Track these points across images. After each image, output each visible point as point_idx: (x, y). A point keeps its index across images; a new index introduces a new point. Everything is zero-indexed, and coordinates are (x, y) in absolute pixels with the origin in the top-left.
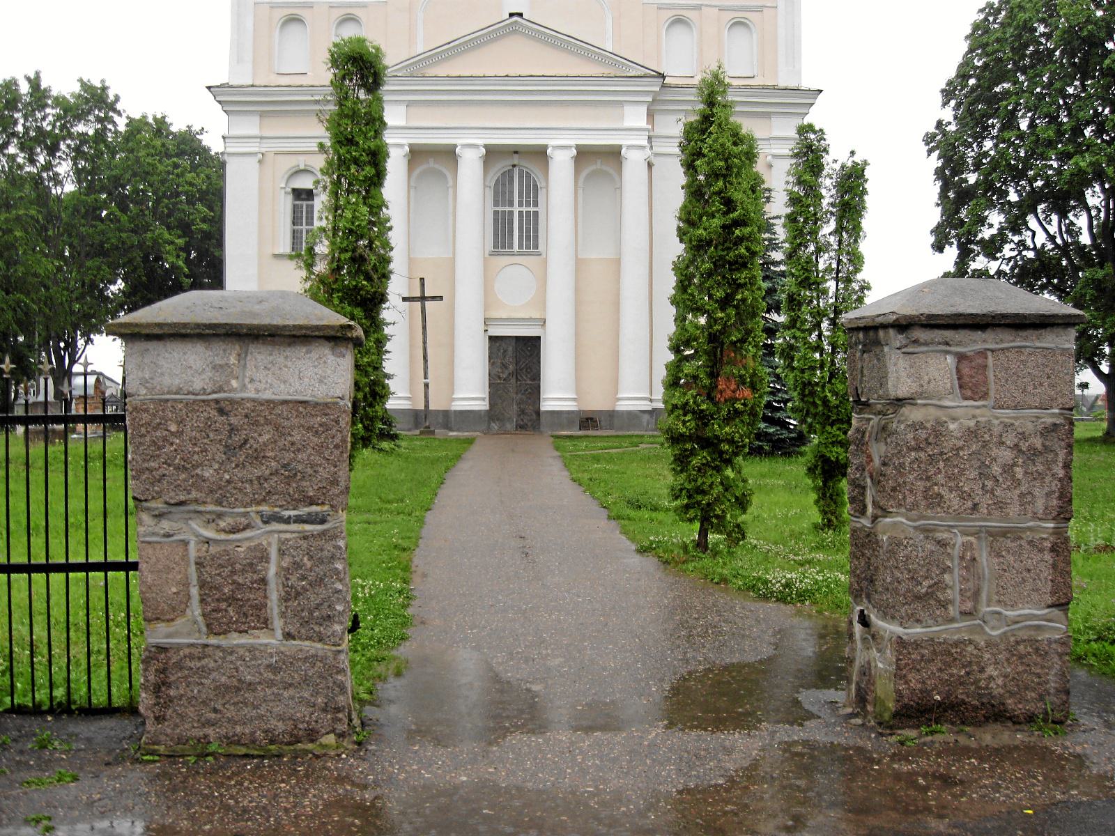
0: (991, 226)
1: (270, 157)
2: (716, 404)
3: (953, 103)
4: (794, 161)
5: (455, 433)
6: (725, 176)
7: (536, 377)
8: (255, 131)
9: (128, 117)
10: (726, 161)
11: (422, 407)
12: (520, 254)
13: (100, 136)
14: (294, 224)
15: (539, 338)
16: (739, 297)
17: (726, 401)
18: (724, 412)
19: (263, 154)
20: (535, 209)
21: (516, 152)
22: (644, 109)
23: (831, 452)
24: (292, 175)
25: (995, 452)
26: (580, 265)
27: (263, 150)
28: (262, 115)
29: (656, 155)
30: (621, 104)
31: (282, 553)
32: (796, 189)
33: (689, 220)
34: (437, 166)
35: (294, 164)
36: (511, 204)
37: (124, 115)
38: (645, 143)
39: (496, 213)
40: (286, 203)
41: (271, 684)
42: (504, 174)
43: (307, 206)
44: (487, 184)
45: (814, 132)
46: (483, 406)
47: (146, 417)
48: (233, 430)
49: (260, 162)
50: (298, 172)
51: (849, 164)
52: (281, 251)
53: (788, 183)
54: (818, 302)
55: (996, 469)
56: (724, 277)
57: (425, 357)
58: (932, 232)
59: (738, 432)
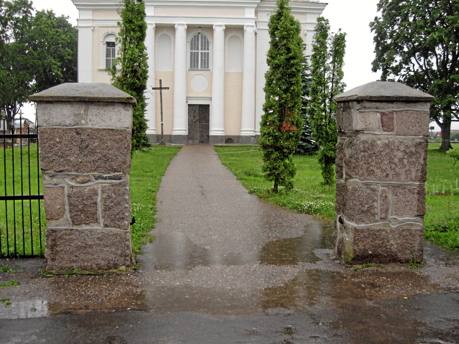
0: (396, 61)
1: (97, 28)
2: (282, 133)
3: (382, 10)
4: (315, 33)
5: (174, 144)
6: (287, 38)
7: (208, 121)
8: (91, 17)
9: (36, 11)
10: (287, 32)
11: (160, 134)
12: (201, 70)
13: (25, 18)
14: (107, 56)
15: (209, 105)
16: (292, 88)
17: (286, 131)
18: (285, 136)
20: (208, 51)
21: (200, 28)
22: (253, 10)
23: (329, 153)
24: (105, 37)
25: (396, 153)
26: (226, 75)
27: (94, 25)
28: (94, 10)
29: (258, 29)
30: (244, 8)
31: (103, 192)
32: (316, 44)
33: (272, 56)
34: (167, 33)
36: (198, 49)
37: (35, 10)
38: (254, 24)
39: (191, 53)
40: (104, 48)
41: (99, 245)
42: (195, 37)
43: (112, 49)
44: (188, 40)
45: (324, 20)
46: (186, 133)
47: (46, 136)
48: (82, 141)
49: (93, 30)
51: (339, 34)
52: (101, 68)
53: (313, 41)
54: (325, 91)
55: (396, 160)
56: (286, 80)
57: (162, 113)
58: (372, 63)
59: (291, 144)
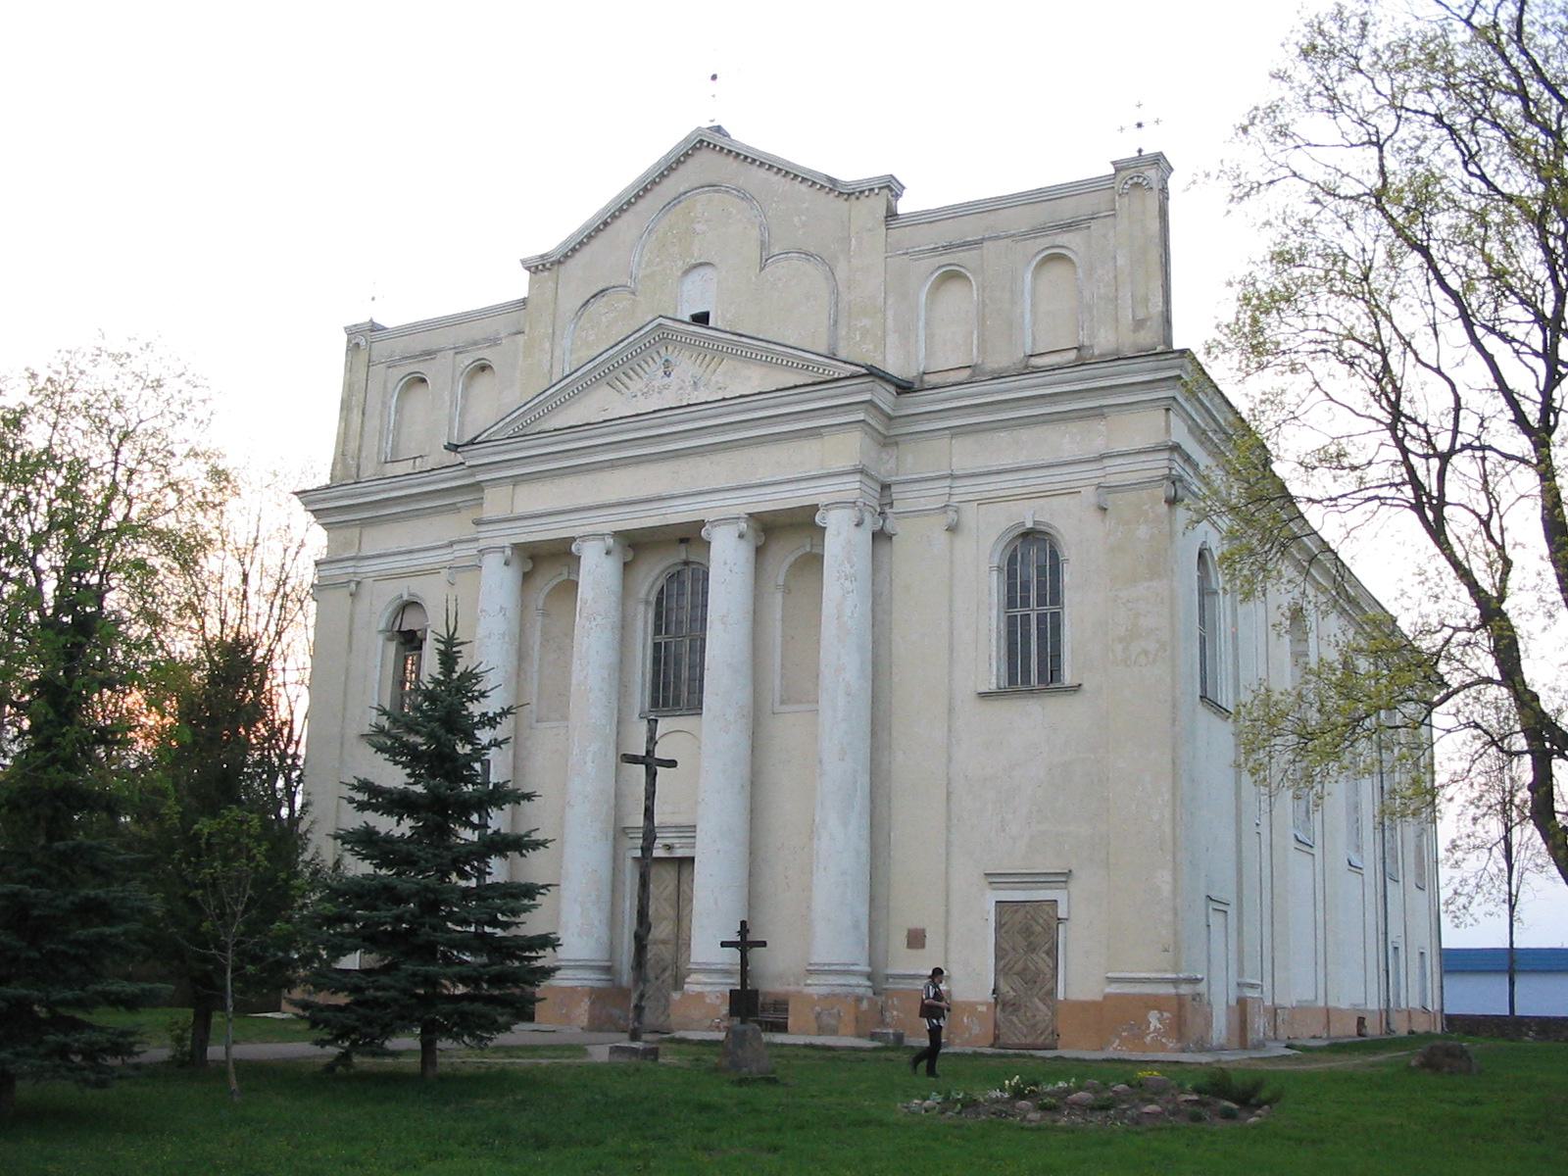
19: (358, 583)
21: (684, 541)
35: (396, 594)
39: (657, 646)
49: (351, 595)
50: (410, 605)
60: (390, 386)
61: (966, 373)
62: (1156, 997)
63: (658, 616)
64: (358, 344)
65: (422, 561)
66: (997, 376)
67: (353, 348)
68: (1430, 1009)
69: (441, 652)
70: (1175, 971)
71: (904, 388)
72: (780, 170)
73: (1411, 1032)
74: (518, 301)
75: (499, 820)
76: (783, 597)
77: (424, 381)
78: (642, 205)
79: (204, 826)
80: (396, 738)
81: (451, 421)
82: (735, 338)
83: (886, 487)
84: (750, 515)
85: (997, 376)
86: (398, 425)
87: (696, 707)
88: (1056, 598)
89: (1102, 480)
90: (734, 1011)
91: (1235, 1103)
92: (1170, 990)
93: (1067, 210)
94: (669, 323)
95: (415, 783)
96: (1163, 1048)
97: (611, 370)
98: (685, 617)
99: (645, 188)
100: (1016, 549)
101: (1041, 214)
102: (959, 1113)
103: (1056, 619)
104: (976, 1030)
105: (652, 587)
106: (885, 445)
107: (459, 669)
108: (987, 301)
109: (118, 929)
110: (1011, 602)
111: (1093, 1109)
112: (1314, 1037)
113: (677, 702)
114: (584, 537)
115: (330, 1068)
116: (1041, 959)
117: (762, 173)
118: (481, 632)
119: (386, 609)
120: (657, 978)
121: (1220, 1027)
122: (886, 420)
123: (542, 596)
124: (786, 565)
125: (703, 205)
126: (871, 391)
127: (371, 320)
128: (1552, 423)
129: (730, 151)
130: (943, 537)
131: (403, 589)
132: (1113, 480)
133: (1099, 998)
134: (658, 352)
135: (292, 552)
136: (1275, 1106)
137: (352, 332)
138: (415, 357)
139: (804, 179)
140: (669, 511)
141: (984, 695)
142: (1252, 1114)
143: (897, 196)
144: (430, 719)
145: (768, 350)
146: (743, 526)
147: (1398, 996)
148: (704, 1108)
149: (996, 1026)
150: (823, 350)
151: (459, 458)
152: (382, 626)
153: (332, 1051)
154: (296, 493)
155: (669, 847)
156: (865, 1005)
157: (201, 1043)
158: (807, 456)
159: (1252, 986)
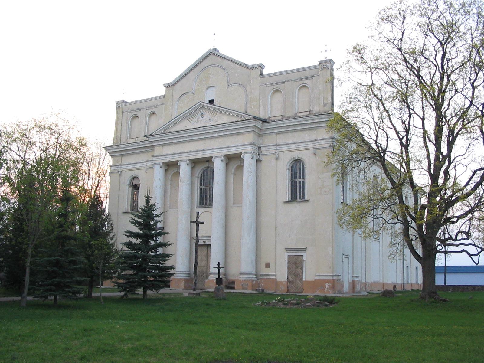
19: (121, 172)
21: (208, 161)
39: (201, 189)
42: (204, 171)
49: (120, 175)
50: (135, 178)
52: (125, 210)
60: (128, 118)
61: (280, 118)
62: (328, 280)
63: (201, 181)
64: (119, 106)
65: (138, 166)
66: (289, 118)
67: (118, 107)
68: (419, 283)
69: (146, 200)
70: (332, 273)
71: (264, 121)
72: (232, 61)
73: (412, 290)
74: (163, 96)
75: (160, 239)
76: (234, 177)
77: (137, 116)
78: (195, 69)
79: (93, 242)
80: (136, 220)
81: (145, 128)
82: (220, 108)
83: (259, 148)
84: (224, 155)
85: (289, 118)
86: (131, 128)
87: (211, 205)
88: (303, 177)
89: (315, 146)
90: (217, 283)
91: (328, 303)
92: (331, 278)
93: (307, 74)
94: (203, 103)
95: (141, 231)
96: (329, 292)
97: (187, 116)
98: (208, 181)
99: (196, 65)
100: (293, 164)
101: (301, 75)
102: (266, 305)
103: (303, 182)
104: (283, 289)
105: (200, 172)
106: (259, 136)
107: (150, 204)
108: (286, 98)
109: (79, 266)
110: (292, 178)
111: (295, 304)
112: (379, 291)
113: (206, 204)
114: (181, 161)
115: (122, 297)
116: (299, 270)
117: (227, 62)
118: (155, 185)
119: (129, 178)
120: (202, 276)
121: (346, 287)
122: (260, 130)
123: (170, 177)
124: (234, 169)
125: (212, 70)
126: (255, 123)
127: (123, 100)
128: (408, 143)
129: (219, 56)
130: (274, 161)
131: (133, 173)
132: (318, 147)
133: (313, 280)
134: (200, 111)
135: (102, 160)
136: (338, 304)
137: (118, 103)
138: (135, 110)
139: (238, 64)
140: (204, 154)
141: (285, 202)
142: (331, 305)
143: (263, 69)
144: (144, 216)
145: (228, 111)
146: (223, 158)
147: (408, 279)
148: (207, 304)
149: (288, 287)
150: (243, 111)
151: (148, 139)
152: (128, 183)
153: (123, 293)
154: (104, 148)
155: (204, 242)
156: (254, 282)
157: (90, 293)
158: (239, 140)
159: (356, 277)
